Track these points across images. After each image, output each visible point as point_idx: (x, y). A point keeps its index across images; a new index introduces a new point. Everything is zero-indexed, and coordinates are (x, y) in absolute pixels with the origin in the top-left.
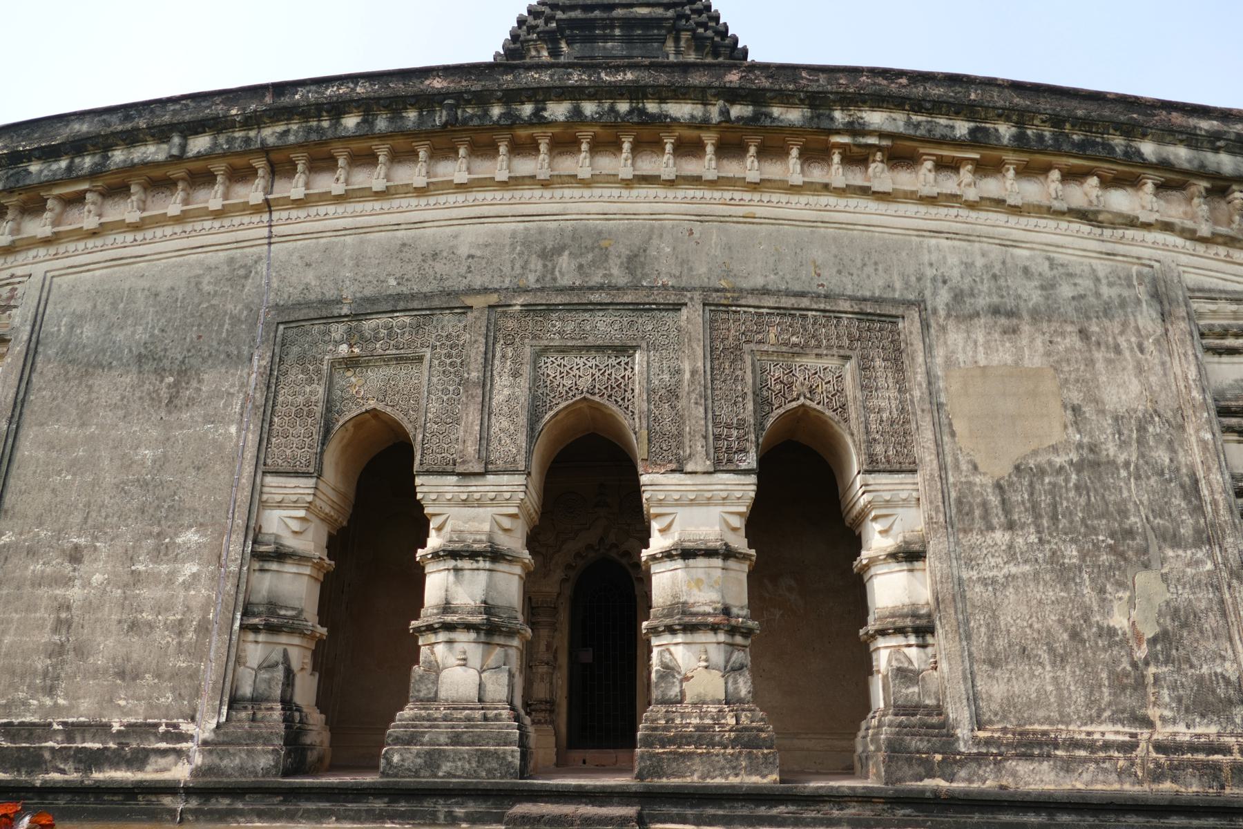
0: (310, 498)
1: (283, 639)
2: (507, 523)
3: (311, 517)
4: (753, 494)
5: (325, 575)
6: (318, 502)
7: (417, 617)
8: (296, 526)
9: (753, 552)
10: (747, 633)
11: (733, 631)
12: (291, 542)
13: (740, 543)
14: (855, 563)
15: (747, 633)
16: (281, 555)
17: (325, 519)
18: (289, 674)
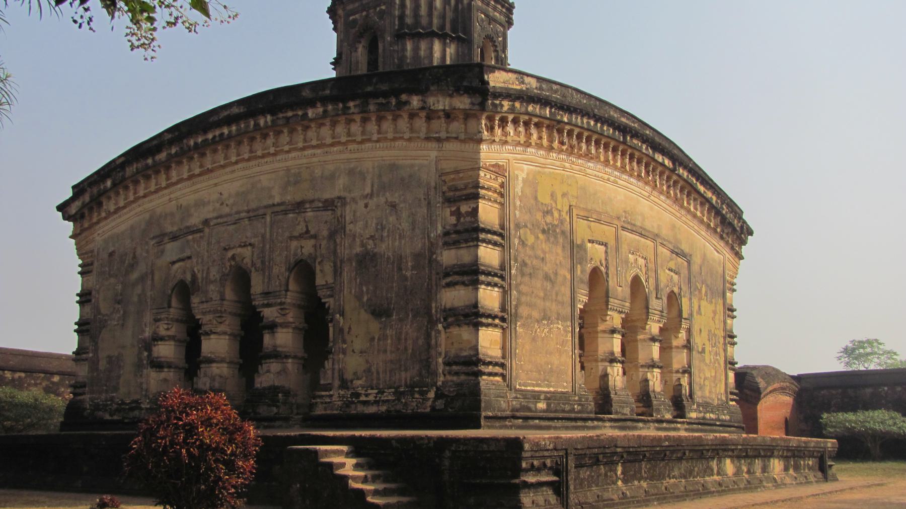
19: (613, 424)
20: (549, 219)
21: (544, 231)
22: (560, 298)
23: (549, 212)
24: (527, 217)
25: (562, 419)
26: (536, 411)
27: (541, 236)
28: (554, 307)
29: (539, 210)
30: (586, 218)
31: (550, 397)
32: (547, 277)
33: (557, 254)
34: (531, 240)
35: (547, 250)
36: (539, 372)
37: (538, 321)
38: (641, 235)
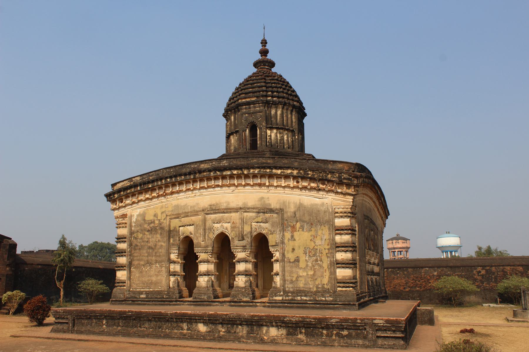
1: (176, 277)
11: (246, 275)
12: (176, 260)
16: (174, 262)
18: (178, 282)
19: (189, 303)
20: (152, 225)
21: (148, 231)
22: (158, 254)
23: (153, 222)
24: (138, 228)
25: (155, 301)
26: (140, 298)
27: (147, 233)
28: (154, 258)
29: (146, 223)
30: (178, 218)
31: (147, 293)
32: (150, 248)
33: (157, 237)
34: (140, 236)
35: (150, 237)
36: (144, 284)
37: (143, 265)
38: (224, 212)
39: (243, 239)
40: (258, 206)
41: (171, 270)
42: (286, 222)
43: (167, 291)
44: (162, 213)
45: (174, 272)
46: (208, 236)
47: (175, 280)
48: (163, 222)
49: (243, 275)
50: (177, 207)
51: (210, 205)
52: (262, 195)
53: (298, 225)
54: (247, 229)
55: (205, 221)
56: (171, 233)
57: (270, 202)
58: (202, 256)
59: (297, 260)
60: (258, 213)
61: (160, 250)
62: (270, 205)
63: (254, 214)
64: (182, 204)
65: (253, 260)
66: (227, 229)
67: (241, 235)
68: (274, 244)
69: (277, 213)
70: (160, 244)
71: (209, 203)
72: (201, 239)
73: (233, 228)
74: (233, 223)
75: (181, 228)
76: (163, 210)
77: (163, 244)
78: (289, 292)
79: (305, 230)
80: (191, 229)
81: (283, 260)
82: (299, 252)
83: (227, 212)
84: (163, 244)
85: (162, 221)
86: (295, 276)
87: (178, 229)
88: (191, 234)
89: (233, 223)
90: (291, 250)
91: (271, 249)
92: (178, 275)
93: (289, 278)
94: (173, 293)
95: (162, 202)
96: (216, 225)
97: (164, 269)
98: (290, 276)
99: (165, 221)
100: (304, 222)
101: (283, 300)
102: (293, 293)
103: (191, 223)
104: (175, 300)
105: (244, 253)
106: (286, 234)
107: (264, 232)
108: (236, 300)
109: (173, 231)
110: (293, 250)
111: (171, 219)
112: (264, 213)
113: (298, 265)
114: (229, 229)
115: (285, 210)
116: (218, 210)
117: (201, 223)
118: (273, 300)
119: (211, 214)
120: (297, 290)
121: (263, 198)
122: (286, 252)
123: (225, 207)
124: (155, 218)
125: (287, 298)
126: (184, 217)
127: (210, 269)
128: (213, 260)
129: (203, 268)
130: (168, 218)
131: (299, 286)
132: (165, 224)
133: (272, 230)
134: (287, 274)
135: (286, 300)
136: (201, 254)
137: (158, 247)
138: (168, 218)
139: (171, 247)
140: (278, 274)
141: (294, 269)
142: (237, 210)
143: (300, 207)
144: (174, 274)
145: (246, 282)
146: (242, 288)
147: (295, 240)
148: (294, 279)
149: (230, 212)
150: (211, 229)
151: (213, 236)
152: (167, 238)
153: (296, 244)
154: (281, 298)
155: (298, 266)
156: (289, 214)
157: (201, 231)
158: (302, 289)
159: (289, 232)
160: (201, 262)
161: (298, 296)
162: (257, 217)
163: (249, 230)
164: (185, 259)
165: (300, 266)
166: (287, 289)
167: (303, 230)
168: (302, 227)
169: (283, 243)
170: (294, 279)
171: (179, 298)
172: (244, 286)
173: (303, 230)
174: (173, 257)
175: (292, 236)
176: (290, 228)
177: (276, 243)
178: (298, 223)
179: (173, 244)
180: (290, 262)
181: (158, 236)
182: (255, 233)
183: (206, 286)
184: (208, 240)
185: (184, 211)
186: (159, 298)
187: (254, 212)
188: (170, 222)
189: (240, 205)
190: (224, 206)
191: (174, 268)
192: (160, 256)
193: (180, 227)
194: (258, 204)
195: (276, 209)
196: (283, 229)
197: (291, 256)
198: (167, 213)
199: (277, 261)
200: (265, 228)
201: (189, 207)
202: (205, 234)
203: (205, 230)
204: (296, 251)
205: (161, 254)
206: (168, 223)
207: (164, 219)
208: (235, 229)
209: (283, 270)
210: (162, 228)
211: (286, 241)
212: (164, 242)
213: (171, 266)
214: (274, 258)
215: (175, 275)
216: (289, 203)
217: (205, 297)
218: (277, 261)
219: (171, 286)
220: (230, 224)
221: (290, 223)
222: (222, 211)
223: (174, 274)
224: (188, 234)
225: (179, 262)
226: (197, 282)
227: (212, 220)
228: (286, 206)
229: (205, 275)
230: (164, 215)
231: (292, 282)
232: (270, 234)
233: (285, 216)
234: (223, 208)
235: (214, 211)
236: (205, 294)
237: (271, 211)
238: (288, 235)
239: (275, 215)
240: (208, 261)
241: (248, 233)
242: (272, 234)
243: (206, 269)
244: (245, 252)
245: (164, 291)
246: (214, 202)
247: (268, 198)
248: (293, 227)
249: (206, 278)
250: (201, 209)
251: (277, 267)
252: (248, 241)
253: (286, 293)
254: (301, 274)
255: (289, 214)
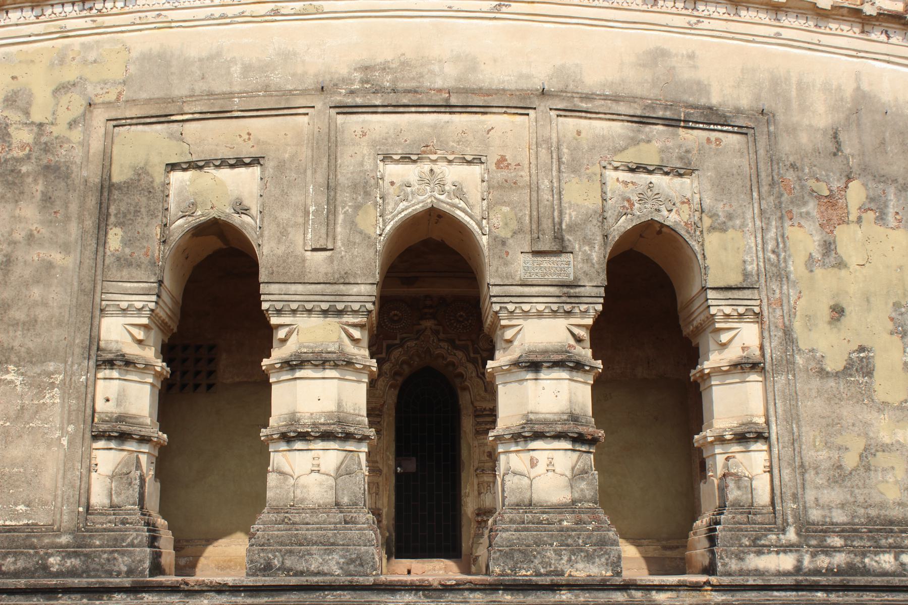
0: (152, 305)
1: (131, 446)
2: (357, 334)
3: (153, 326)
4: (599, 308)
5: (162, 382)
6: (158, 311)
7: (266, 425)
8: (140, 334)
9: (599, 364)
10: (593, 441)
11: (579, 439)
12: (132, 350)
13: (585, 353)
14: (693, 372)
15: (593, 441)
17: (163, 326)
30: (164, 119)
33: (16, 219)
38: (448, 108)
39: (561, 250)
40: (639, 91)
41: (100, 406)
42: (790, 176)
43: (75, 532)
44: (62, 89)
45: (121, 419)
46: (352, 224)
47: (127, 464)
48: (62, 141)
49: (558, 436)
50: (160, 62)
51: (366, 68)
52: (655, 39)
53: (856, 194)
54: (579, 198)
55: (329, 146)
56: (110, 199)
57: (702, 75)
58: (301, 331)
59: (861, 366)
60: (643, 121)
61: (36, 292)
62: (702, 87)
63: (618, 128)
64: (193, 53)
65: (599, 364)
66: (459, 192)
67: (547, 224)
68: (734, 279)
69: (742, 131)
70: (35, 255)
71: (362, 56)
72: (301, 240)
73: (498, 190)
74: (502, 162)
75: (177, 178)
76: (70, 74)
77: (57, 257)
78: (827, 529)
79: (891, 220)
80: (243, 183)
81: (789, 365)
82: (871, 326)
83: (465, 108)
84: (57, 257)
85: (60, 130)
86: (858, 445)
87: (159, 178)
88: (245, 211)
89: (502, 162)
90: (825, 313)
91: (719, 306)
92: (144, 440)
93: (823, 454)
94: (116, 543)
95: (64, 34)
96: (394, 171)
97: (53, 398)
98: (827, 445)
99: (76, 135)
100: (883, 179)
101: (798, 570)
102: (849, 531)
103: (247, 152)
104: (127, 582)
105: (562, 323)
106: (793, 232)
107: (672, 219)
108: (525, 574)
109: (127, 187)
110: (838, 312)
111: (118, 122)
112: (672, 123)
113: (869, 387)
114: (475, 192)
115: (780, 117)
116: (415, 91)
117: (305, 153)
118: (741, 573)
119: (372, 109)
120: (870, 520)
121: (659, 55)
122: (797, 325)
123: (450, 83)
124: (14, 116)
125: (823, 561)
126: (204, 116)
127: (349, 408)
128: (361, 354)
129: (301, 397)
130: (99, 117)
131: (877, 499)
132: (82, 147)
133: (721, 209)
134: (809, 435)
135: (817, 572)
136: (301, 321)
137: (19, 271)
138: (99, 117)
139: (114, 273)
140: (761, 436)
141: (847, 412)
142: (521, 102)
143: (860, 107)
144: (119, 433)
145: (578, 475)
146: (559, 508)
147: (841, 264)
148: (850, 461)
149: (484, 109)
150: (366, 188)
151: (380, 225)
152: (89, 223)
153: (851, 284)
154: (787, 562)
155: (866, 396)
156: (804, 138)
157: (311, 196)
158: (896, 513)
159: (811, 227)
160: (291, 365)
161: (879, 549)
162: (635, 142)
163: (593, 202)
164: (168, 352)
165: (880, 395)
166: (815, 515)
167: (881, 218)
168: (876, 207)
169: (781, 275)
170: (850, 461)
171: (152, 574)
172: (562, 496)
173: (881, 218)
174: (116, 332)
175: (828, 247)
176: (812, 207)
177: (746, 275)
178: (854, 185)
179: (124, 262)
180: (822, 373)
181: (29, 211)
182: (624, 224)
183: (330, 498)
184: (349, 244)
185: (200, 87)
186: (16, 574)
187: (615, 117)
188: (109, 139)
189: (540, 74)
190: (444, 76)
191: (121, 398)
192: (31, 324)
193: (173, 167)
194: (641, 84)
195: (738, 112)
196: (779, 206)
197: (829, 345)
198: (90, 90)
199: (747, 366)
200: (676, 201)
201: (236, 70)
202: (332, 212)
203: (330, 188)
204: (852, 318)
205: (42, 314)
206: (96, 145)
207: (72, 124)
208: (515, 197)
209: (792, 417)
210: (54, 172)
211: (796, 267)
212: (66, 248)
213: (100, 384)
214: (714, 360)
215: (123, 437)
216: (802, 88)
217: (332, 565)
218: (747, 366)
219: (98, 498)
220: (477, 169)
221: (811, 183)
222: (438, 99)
223: (119, 433)
224: (224, 211)
225: (148, 366)
226: (272, 479)
227: (373, 144)
228: (788, 102)
229: (327, 436)
230: (75, 103)
231: (839, 475)
232: (712, 229)
233: (785, 145)
234: (439, 83)
235: (392, 99)
236: (329, 545)
237: (714, 118)
238: (804, 239)
239: (732, 140)
240: (344, 363)
241: (587, 220)
242: (722, 228)
243: (332, 407)
244: (569, 313)
245: (53, 530)
246: (384, 54)
247: (691, 56)
248: (831, 201)
249: (330, 456)
250: (309, 83)
251: (730, 403)
252: (587, 260)
253: (814, 534)
254: (885, 438)
255: (804, 138)
